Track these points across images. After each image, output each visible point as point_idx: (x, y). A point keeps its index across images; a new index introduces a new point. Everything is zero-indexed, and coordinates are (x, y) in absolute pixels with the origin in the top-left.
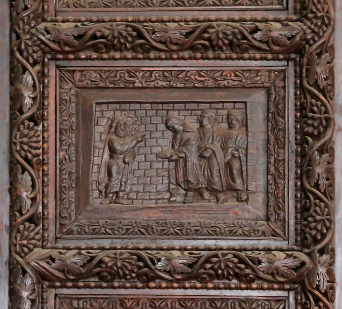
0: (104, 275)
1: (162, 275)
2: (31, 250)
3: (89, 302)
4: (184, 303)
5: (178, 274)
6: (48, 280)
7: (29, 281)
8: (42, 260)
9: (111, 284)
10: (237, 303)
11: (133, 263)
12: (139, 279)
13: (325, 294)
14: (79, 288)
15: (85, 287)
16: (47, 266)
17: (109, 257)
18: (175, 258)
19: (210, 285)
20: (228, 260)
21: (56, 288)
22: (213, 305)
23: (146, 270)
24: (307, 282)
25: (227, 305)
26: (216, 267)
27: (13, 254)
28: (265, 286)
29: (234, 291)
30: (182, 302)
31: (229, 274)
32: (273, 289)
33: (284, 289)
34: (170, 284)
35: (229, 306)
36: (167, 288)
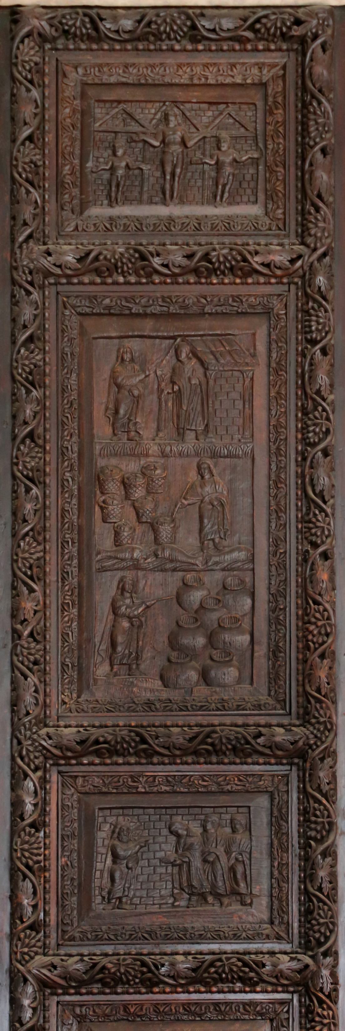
1: (166, 980)
2: (32, 958)
3: (92, 1009)
5: (182, 978)
7: (30, 989)
8: (43, 967)
9: (114, 990)
10: (241, 1006)
11: (137, 968)
12: (142, 984)
13: (329, 996)
14: (81, 994)
15: (88, 993)
17: (111, 963)
18: (179, 963)
19: (214, 989)
20: (232, 964)
21: (58, 995)
23: (149, 975)
24: (310, 985)
25: (231, 1008)
26: (220, 971)
27: (14, 962)
28: (270, 989)
29: (238, 994)
31: (233, 977)
32: (277, 992)
33: (288, 992)
34: (174, 989)
35: (234, 1009)
36: (171, 992)
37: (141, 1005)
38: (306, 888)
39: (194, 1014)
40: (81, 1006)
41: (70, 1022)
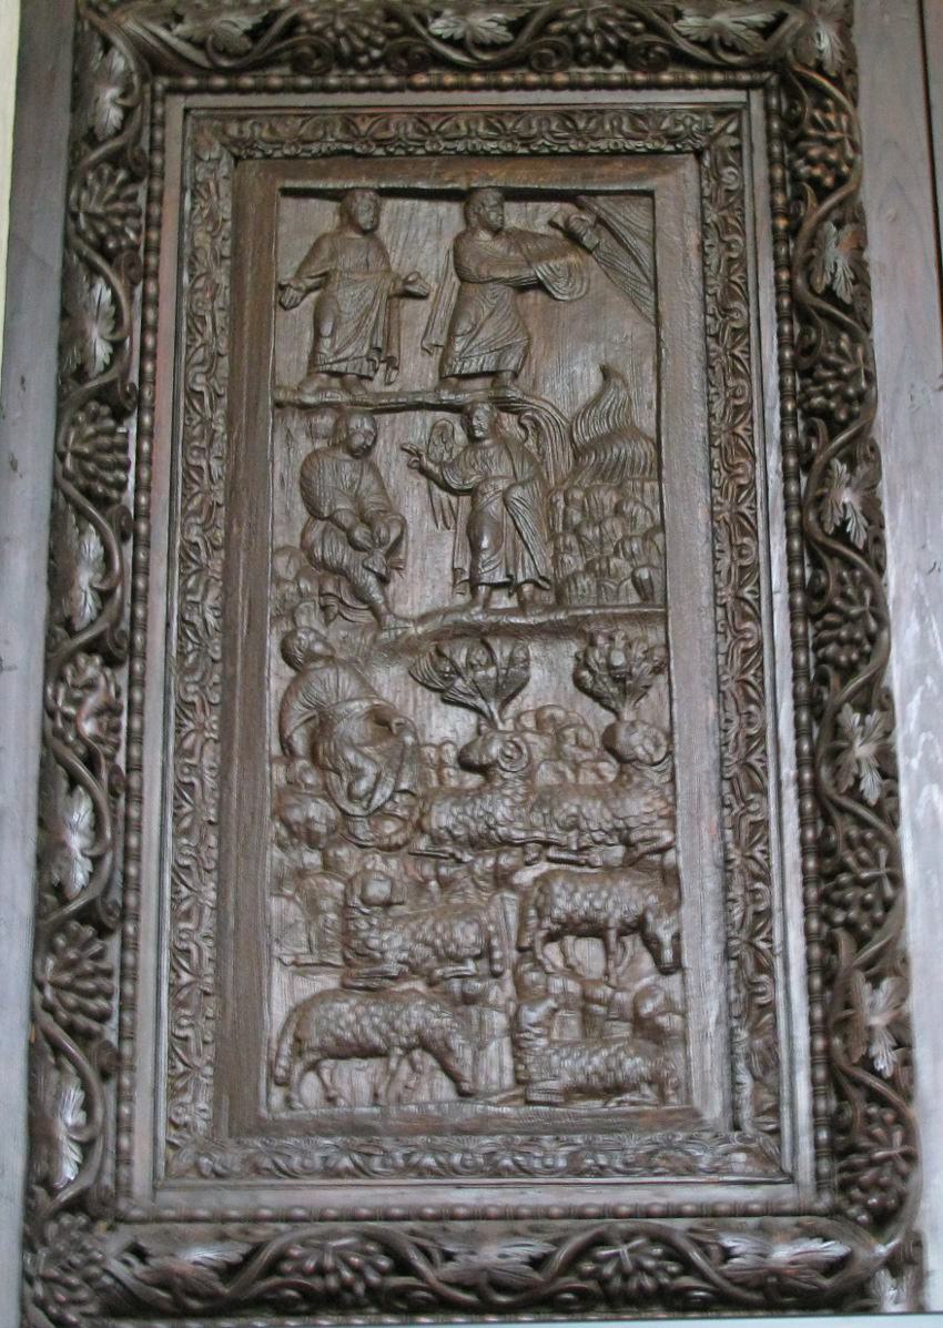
0: (303, 54)
4: (500, 122)
6: (170, 73)
10: (625, 119)
12: (388, 67)
13: (837, 82)
14: (244, 91)
16: (163, 33)
19: (560, 78)
22: (568, 123)
30: (492, 120)
33: (738, 86)
37: (381, 115)
38: (816, 781)
39: (512, 136)
40: (242, 120)
41: (214, 155)
